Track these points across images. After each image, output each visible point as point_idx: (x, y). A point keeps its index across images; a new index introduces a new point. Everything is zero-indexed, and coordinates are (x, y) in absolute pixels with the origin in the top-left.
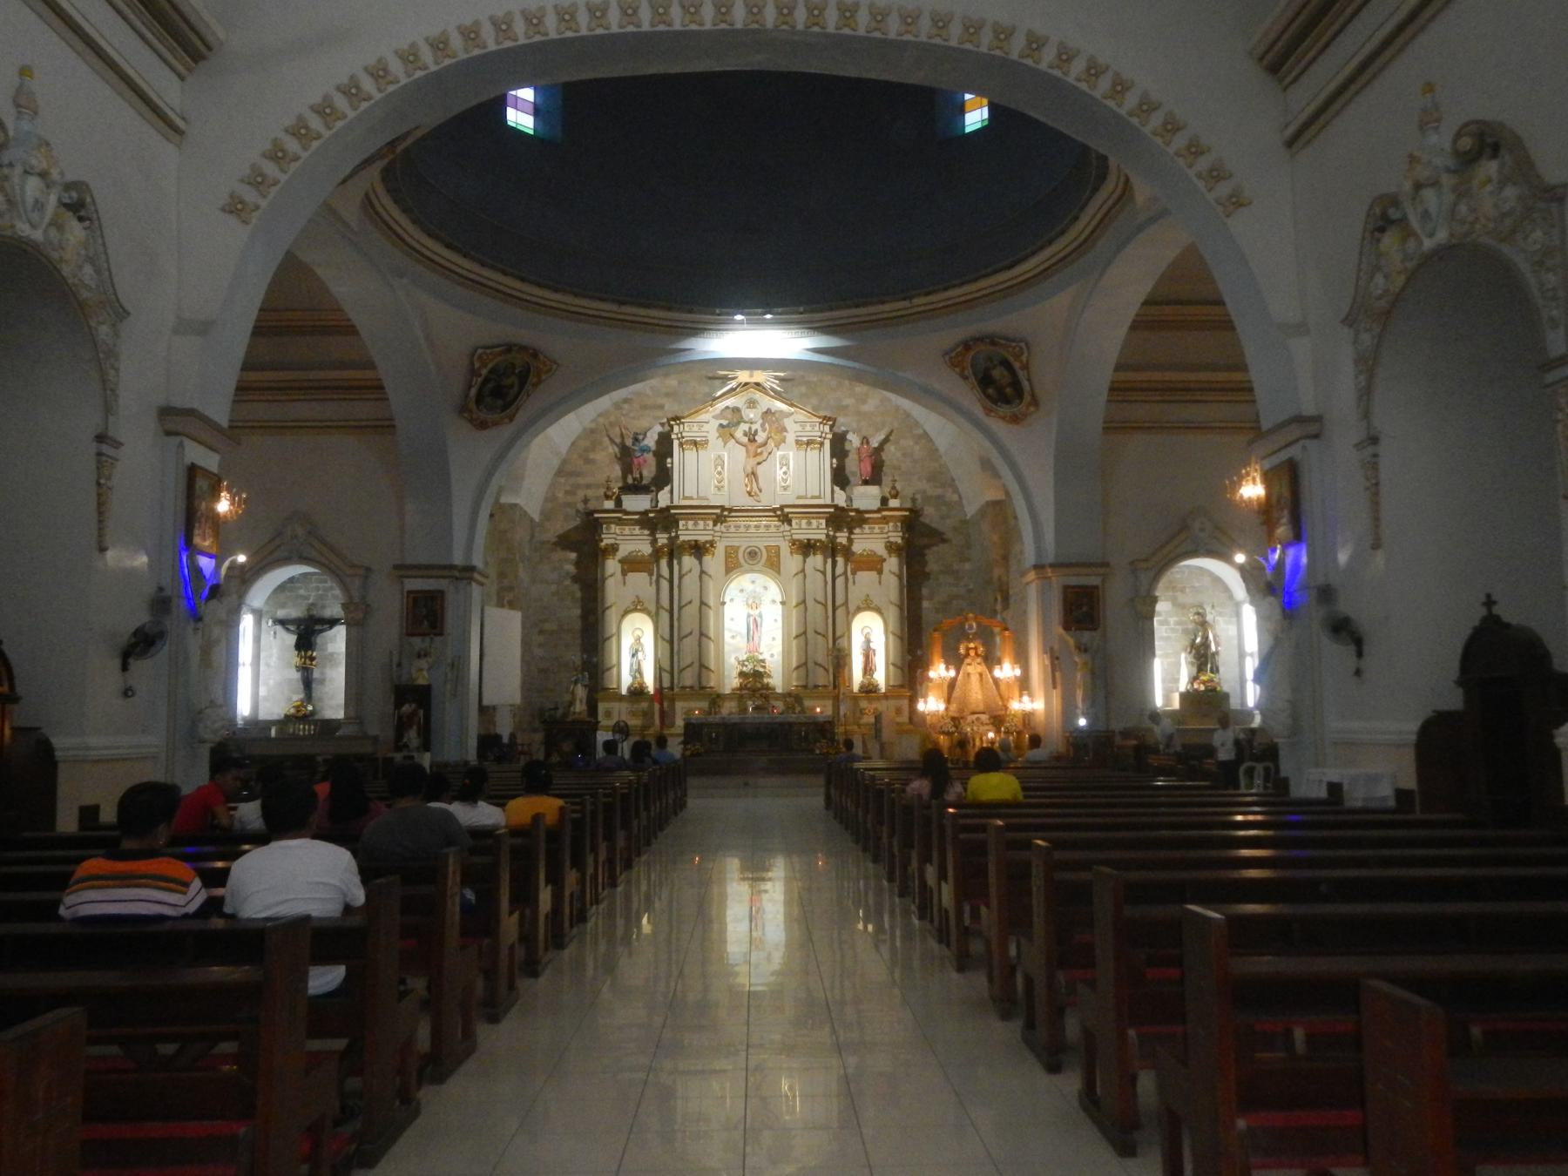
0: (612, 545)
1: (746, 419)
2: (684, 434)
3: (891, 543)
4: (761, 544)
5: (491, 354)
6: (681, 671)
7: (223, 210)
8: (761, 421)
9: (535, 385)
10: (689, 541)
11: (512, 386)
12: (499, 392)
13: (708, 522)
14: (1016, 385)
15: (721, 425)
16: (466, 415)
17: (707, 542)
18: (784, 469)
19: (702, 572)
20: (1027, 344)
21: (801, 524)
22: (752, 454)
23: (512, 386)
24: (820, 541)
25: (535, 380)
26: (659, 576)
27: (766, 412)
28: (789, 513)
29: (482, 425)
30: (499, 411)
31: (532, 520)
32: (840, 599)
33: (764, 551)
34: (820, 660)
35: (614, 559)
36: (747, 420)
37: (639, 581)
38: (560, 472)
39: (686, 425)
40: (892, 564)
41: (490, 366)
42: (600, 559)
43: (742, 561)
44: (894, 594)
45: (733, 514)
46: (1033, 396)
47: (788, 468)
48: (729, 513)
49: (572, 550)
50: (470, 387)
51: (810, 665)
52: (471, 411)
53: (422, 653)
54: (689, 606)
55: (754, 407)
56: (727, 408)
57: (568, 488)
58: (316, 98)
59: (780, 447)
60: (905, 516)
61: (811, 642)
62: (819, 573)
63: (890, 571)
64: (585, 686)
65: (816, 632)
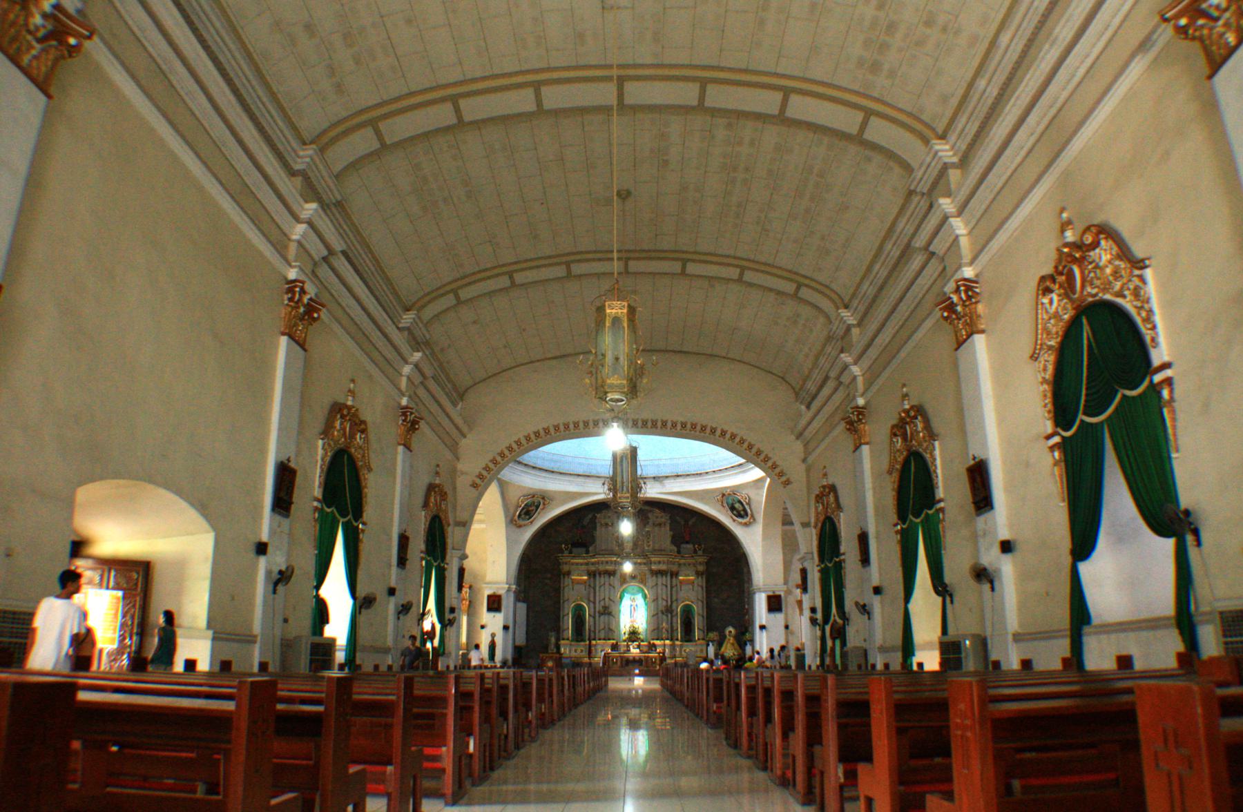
6: (599, 632)
7: (471, 485)
9: (543, 509)
14: (745, 510)
19: (610, 585)
26: (590, 586)
29: (520, 526)
32: (674, 598)
40: (701, 581)
43: (628, 580)
46: (752, 516)
58: (499, 451)
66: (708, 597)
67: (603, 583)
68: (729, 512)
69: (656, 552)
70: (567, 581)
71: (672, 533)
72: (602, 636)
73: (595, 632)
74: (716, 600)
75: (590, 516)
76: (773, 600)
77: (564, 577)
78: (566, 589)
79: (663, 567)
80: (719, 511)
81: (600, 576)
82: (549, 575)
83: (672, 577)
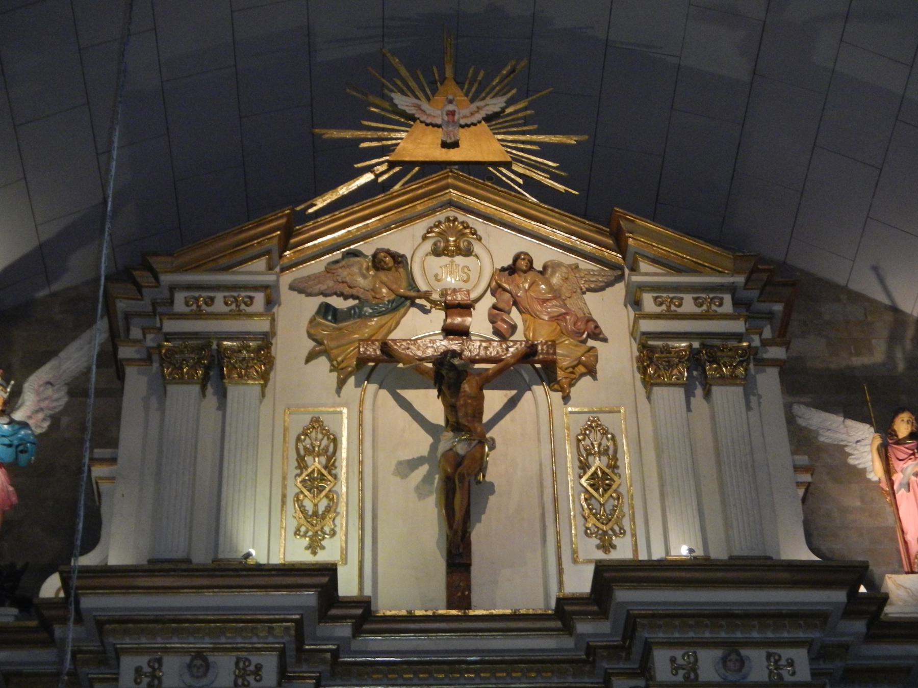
1: (423, 286)
2: (170, 326)
8: (489, 300)
13: (255, 659)
15: (326, 310)
18: (597, 463)
21: (694, 667)
27: (512, 270)
36: (435, 296)
39: (180, 297)
45: (375, 641)
47: (614, 467)
48: (358, 631)
55: (468, 253)
56: (356, 254)
59: (574, 391)
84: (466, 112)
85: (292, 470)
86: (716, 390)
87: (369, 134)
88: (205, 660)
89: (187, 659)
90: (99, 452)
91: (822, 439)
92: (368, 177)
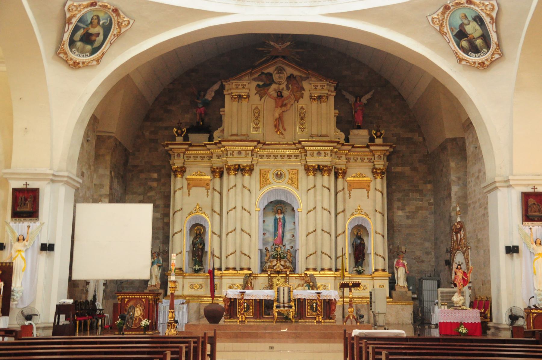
0: (181, 168)
1: (275, 80)
3: (376, 169)
4: (284, 169)
5: (80, 5)
6: (227, 257)
8: (286, 83)
9: (119, 35)
10: (235, 165)
11: (98, 35)
12: (87, 38)
13: (248, 152)
14: (485, 38)
16: (62, 55)
17: (247, 166)
20: (498, 4)
22: (280, 104)
23: (98, 35)
24: (326, 166)
25: (115, 32)
26: (214, 189)
28: (303, 147)
29: (76, 65)
30: (89, 55)
31: (126, 150)
32: (340, 209)
33: (287, 173)
34: (326, 250)
35: (182, 177)
37: (199, 193)
38: (147, 118)
41: (78, 16)
42: (173, 177)
44: (379, 207)
46: (499, 45)
47: (305, 116)
49: (153, 173)
50: (64, 32)
51: (319, 253)
52: (66, 53)
53: (21, 238)
54: (234, 210)
56: (263, 73)
57: (153, 129)
60: (387, 151)
61: (319, 237)
62: (326, 190)
63: (376, 189)
64: (159, 266)
65: (323, 230)
66: (389, 209)
67: (232, 184)
68: (453, 45)
69: (314, 138)
70: (178, 182)
71: (337, 111)
72: (231, 265)
73: (220, 258)
74: (400, 213)
75: (216, 87)
76: (531, 201)
77: (176, 176)
78: (178, 194)
79: (325, 161)
80: (431, 46)
81: (229, 174)
82: (155, 175)
83: (336, 177)
84: (283, 45)
85: (253, 116)
86: (322, 103)
87: (266, 49)
88: (240, 152)
89: (238, 152)
90: (221, 110)
91: (346, 97)
92: (265, 58)
